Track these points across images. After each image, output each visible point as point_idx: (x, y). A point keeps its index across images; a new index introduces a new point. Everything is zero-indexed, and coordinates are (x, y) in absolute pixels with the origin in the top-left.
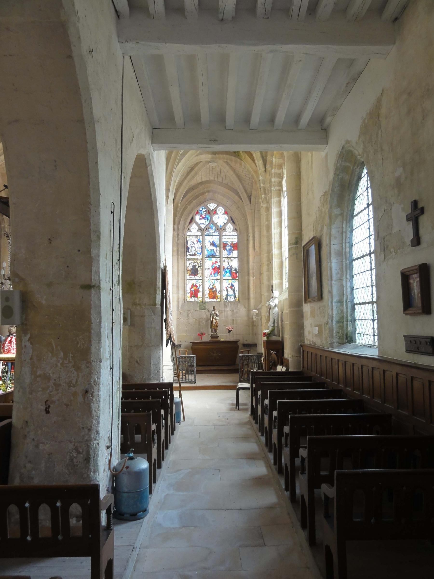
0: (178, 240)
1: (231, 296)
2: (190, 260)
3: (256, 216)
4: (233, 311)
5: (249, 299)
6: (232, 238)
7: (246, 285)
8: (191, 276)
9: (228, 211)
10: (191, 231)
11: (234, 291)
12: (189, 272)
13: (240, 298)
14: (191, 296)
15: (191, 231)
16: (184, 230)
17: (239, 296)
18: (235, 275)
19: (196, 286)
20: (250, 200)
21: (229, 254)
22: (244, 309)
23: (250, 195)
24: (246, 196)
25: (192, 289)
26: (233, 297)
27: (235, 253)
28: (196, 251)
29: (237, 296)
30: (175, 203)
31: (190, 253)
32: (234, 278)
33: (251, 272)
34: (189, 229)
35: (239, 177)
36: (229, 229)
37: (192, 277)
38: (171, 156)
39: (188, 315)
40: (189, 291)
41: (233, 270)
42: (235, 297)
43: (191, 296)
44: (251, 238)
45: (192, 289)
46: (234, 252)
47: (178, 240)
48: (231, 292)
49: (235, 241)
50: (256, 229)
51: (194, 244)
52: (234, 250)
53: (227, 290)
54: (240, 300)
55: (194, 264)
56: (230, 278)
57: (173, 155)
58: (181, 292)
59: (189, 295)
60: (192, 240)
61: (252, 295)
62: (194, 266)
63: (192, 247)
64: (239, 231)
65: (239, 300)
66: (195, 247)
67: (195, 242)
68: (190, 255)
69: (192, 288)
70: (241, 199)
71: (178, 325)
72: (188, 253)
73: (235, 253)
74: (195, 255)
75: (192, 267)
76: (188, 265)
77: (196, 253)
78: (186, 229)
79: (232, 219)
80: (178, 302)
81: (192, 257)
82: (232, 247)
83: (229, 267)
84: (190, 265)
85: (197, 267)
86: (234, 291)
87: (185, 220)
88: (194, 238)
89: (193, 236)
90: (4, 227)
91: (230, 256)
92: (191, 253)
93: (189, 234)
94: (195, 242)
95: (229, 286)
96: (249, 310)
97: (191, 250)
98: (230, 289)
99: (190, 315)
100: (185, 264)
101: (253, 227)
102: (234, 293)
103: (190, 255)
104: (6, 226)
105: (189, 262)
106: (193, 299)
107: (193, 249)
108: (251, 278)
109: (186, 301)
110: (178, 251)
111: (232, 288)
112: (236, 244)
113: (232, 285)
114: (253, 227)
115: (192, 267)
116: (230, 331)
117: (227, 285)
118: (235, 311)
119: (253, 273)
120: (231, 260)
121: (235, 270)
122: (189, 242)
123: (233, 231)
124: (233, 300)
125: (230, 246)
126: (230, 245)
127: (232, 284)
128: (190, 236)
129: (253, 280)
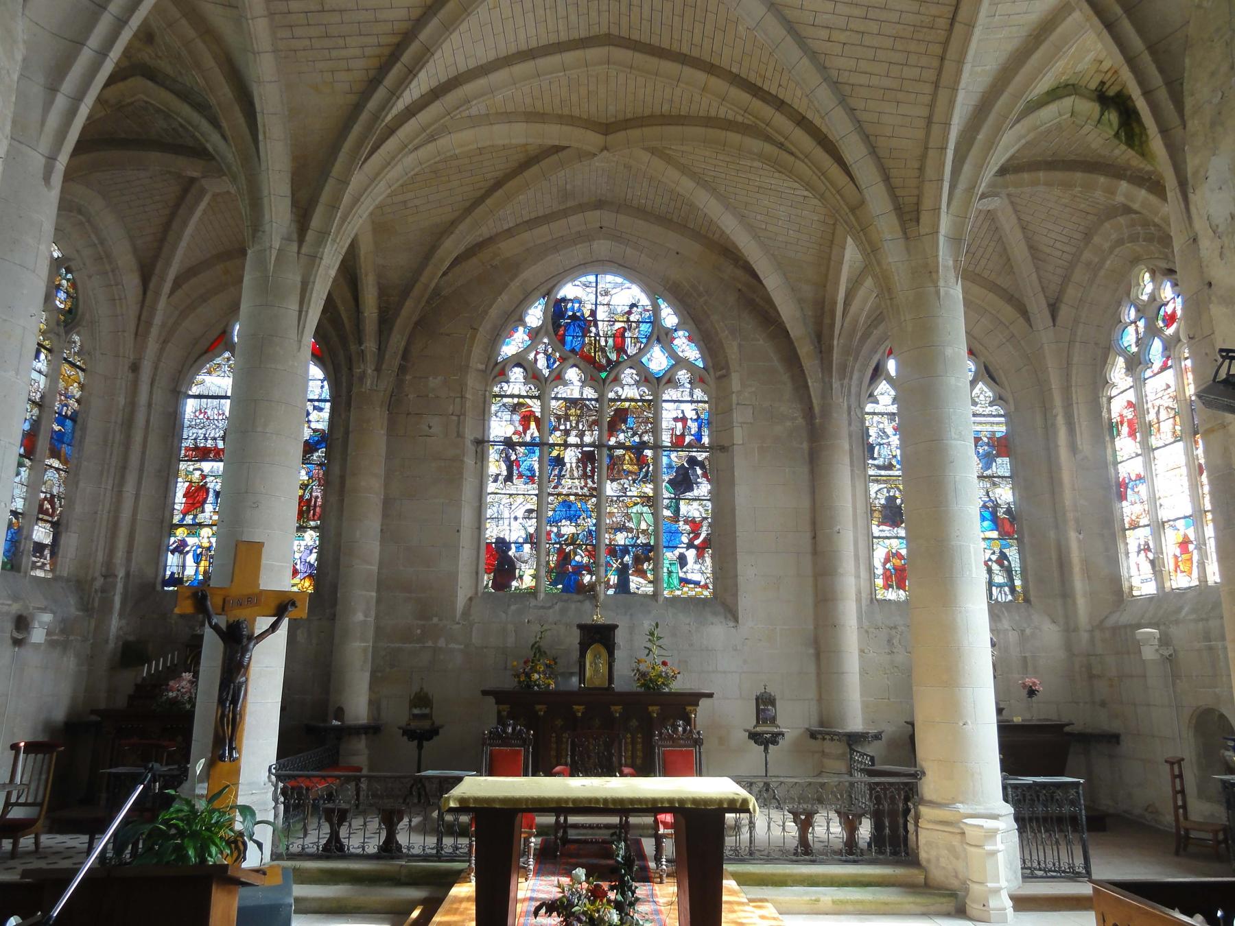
0: (850, 424)
1: (1000, 586)
2: (877, 481)
3: (1075, 359)
4: (1023, 631)
5: (1066, 594)
6: (992, 424)
7: (1054, 556)
8: (882, 527)
9: (977, 347)
10: (877, 402)
11: (1009, 571)
12: (876, 514)
13: (1032, 593)
14: (887, 586)
15: (877, 402)
16: (859, 395)
17: (1025, 587)
18: (1007, 525)
19: (898, 555)
20: (1054, 318)
21: (988, 466)
22: (1054, 628)
23: (1052, 301)
24: (1044, 304)
25: (888, 566)
26: (1007, 589)
27: (1002, 466)
28: (895, 457)
29: (1019, 589)
30: (848, 320)
31: (876, 462)
32: (1004, 535)
33: (1070, 516)
34: (871, 395)
35: (1033, 248)
36: (982, 397)
37: (887, 530)
38: (975, 138)
39: (889, 641)
40: (879, 571)
41: (1001, 513)
42: (1013, 590)
43: (887, 586)
44: (1060, 420)
45: (888, 566)
46: (999, 460)
47: (850, 424)
48: (999, 578)
49: (1001, 430)
50: (1079, 396)
51: (888, 437)
52: (998, 455)
53: (990, 571)
54: (1032, 599)
55: (888, 492)
56: (995, 534)
57: (980, 137)
58: (864, 574)
59: (880, 582)
60: (881, 426)
61: (1079, 585)
62: (891, 499)
63: (880, 444)
64: (1011, 401)
65: (1027, 600)
66: (889, 444)
67: (890, 431)
68: (879, 467)
69: (887, 560)
70: (1024, 312)
71: (864, 672)
72: (870, 461)
73: (1002, 466)
74: (890, 467)
75: (883, 501)
76: (873, 495)
77: (894, 462)
78: (864, 395)
79: (986, 368)
80: (859, 600)
81: (883, 473)
82: (993, 446)
83: (990, 504)
84: (878, 493)
85: (898, 501)
86: (1009, 571)
87: (863, 372)
88: (885, 419)
89: (882, 414)
90: (363, 377)
91: (989, 472)
92: (880, 462)
93: (869, 408)
94: (890, 431)
95: (994, 558)
96: (1069, 629)
97: (879, 454)
98: (995, 567)
99: (895, 641)
100: (867, 491)
101: (1067, 390)
102: (1011, 580)
103: (879, 467)
104: (369, 371)
105: (874, 488)
106: (892, 595)
107: (885, 451)
108: (1073, 535)
109: (873, 600)
110: (851, 451)
111: (1001, 565)
112: (1005, 437)
113: (1003, 556)
114: (1067, 390)
115: (883, 501)
116: (1032, 693)
117: (988, 554)
118: (1028, 631)
119: (1077, 521)
120: (994, 484)
121: (1009, 511)
122: (872, 432)
123: (991, 404)
124: (1010, 597)
125: (988, 444)
126: (985, 440)
127: (1001, 552)
128: (874, 413)
129: (1079, 541)
